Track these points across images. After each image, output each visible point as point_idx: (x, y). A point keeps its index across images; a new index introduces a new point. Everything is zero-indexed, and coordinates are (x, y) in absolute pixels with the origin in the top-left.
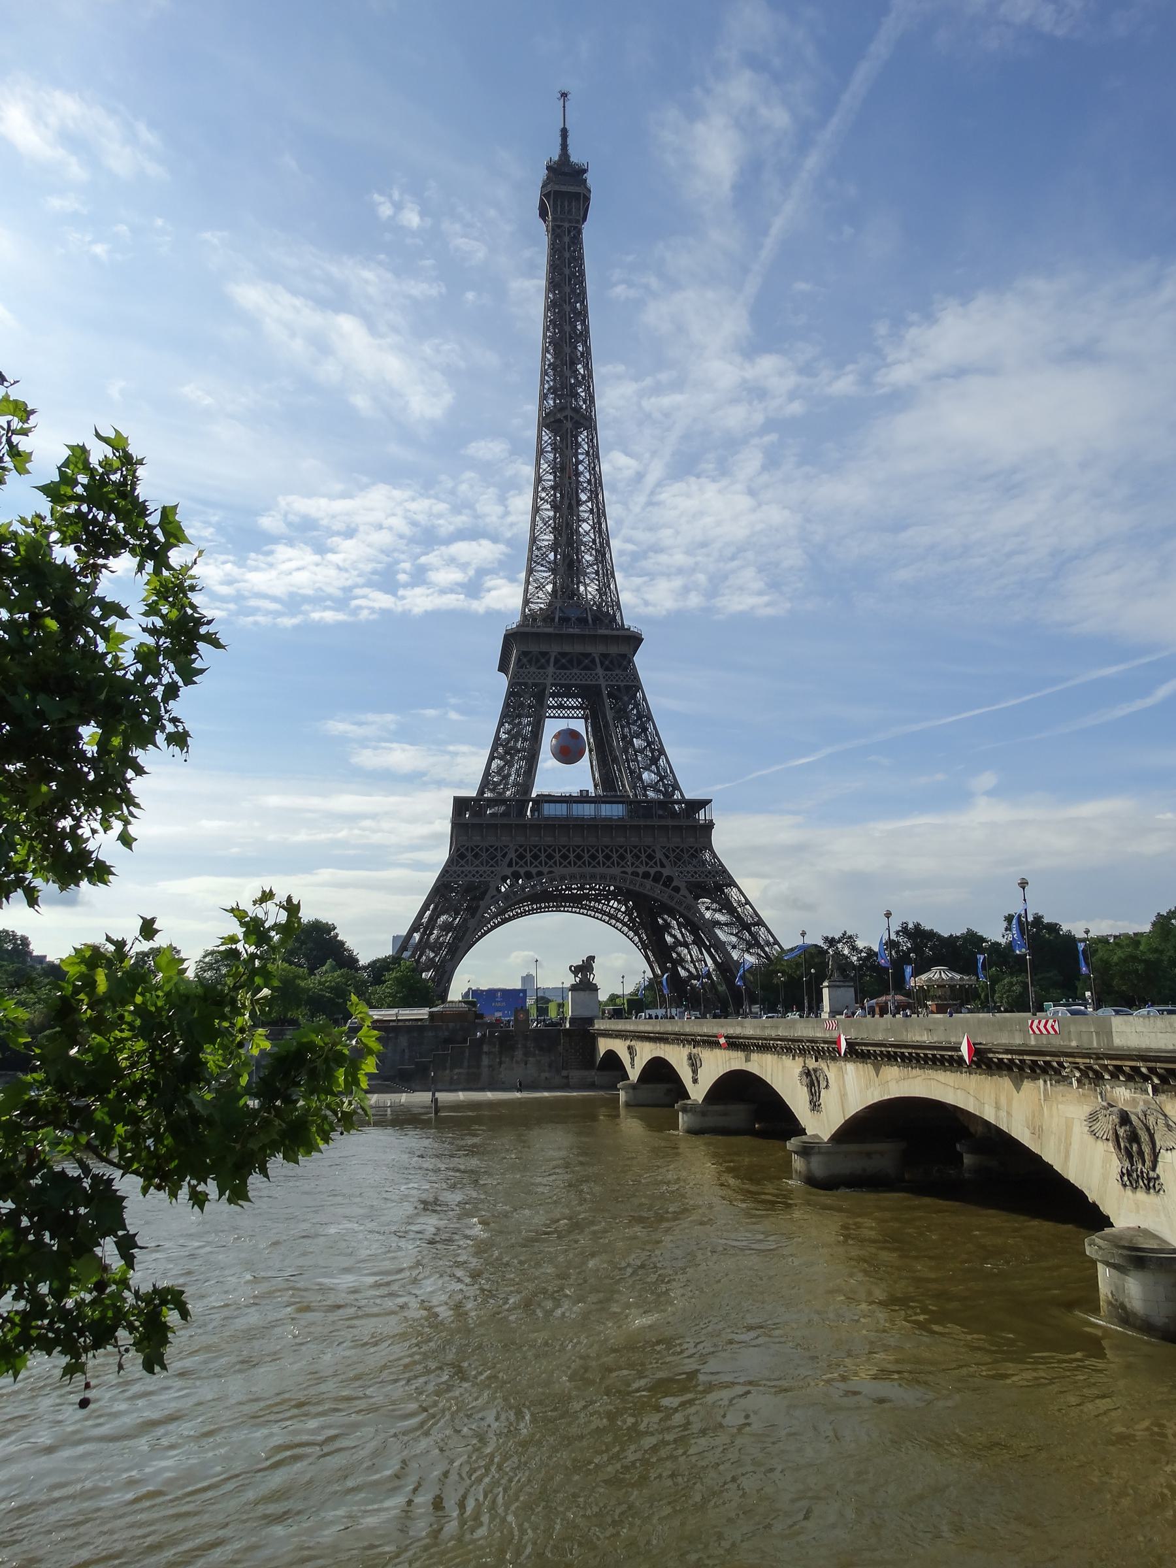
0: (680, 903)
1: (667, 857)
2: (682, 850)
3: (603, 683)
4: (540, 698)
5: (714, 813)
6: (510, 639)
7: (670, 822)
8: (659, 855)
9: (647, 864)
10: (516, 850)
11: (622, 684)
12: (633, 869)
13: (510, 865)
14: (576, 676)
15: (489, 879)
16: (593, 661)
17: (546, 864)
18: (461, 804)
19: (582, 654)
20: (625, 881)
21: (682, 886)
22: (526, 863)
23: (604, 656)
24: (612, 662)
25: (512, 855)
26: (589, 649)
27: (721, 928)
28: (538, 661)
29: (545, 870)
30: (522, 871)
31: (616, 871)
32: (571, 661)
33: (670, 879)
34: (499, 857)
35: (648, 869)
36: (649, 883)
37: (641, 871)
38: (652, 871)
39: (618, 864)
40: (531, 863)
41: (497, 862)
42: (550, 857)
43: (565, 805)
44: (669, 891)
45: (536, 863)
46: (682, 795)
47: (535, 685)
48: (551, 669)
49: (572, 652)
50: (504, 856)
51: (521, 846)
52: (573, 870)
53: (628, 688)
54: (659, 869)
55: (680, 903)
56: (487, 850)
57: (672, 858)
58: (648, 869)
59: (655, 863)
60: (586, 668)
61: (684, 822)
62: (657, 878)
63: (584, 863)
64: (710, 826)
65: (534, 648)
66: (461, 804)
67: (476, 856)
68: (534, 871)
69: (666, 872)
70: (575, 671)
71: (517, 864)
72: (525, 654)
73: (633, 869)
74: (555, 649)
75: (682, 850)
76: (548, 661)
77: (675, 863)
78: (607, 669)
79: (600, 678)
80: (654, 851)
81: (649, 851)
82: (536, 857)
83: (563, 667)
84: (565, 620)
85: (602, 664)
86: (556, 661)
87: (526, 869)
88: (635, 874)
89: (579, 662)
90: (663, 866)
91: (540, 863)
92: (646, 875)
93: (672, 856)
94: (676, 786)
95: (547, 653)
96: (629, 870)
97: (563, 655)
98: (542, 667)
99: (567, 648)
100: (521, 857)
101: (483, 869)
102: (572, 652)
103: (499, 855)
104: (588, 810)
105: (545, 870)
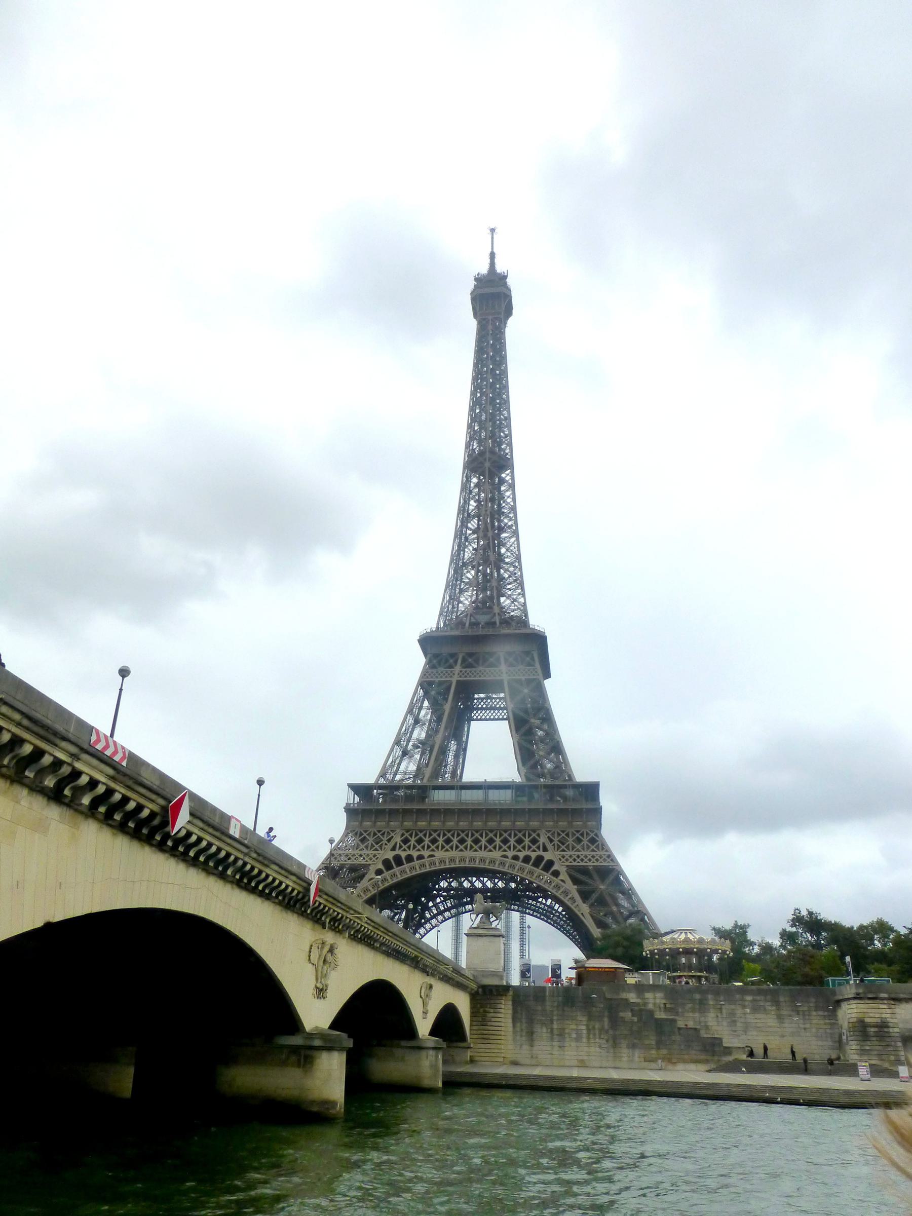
1: (551, 841)
8: (543, 840)
10: (403, 835)
12: (515, 853)
13: (393, 849)
21: (563, 870)
25: (398, 839)
29: (426, 853)
30: (403, 855)
31: (497, 855)
33: (550, 863)
36: (529, 867)
37: (521, 855)
38: (533, 855)
39: (500, 848)
41: (381, 847)
43: (453, 792)
45: (419, 847)
50: (389, 841)
52: (454, 853)
54: (541, 853)
55: (558, 887)
56: (375, 834)
59: (538, 848)
68: (415, 854)
69: (547, 856)
71: (401, 847)
77: (559, 847)
80: (538, 835)
81: (534, 835)
87: (408, 852)
90: (545, 849)
91: (423, 847)
92: (527, 859)
93: (556, 840)
96: (510, 854)
100: (406, 841)
103: (385, 839)
105: (426, 853)
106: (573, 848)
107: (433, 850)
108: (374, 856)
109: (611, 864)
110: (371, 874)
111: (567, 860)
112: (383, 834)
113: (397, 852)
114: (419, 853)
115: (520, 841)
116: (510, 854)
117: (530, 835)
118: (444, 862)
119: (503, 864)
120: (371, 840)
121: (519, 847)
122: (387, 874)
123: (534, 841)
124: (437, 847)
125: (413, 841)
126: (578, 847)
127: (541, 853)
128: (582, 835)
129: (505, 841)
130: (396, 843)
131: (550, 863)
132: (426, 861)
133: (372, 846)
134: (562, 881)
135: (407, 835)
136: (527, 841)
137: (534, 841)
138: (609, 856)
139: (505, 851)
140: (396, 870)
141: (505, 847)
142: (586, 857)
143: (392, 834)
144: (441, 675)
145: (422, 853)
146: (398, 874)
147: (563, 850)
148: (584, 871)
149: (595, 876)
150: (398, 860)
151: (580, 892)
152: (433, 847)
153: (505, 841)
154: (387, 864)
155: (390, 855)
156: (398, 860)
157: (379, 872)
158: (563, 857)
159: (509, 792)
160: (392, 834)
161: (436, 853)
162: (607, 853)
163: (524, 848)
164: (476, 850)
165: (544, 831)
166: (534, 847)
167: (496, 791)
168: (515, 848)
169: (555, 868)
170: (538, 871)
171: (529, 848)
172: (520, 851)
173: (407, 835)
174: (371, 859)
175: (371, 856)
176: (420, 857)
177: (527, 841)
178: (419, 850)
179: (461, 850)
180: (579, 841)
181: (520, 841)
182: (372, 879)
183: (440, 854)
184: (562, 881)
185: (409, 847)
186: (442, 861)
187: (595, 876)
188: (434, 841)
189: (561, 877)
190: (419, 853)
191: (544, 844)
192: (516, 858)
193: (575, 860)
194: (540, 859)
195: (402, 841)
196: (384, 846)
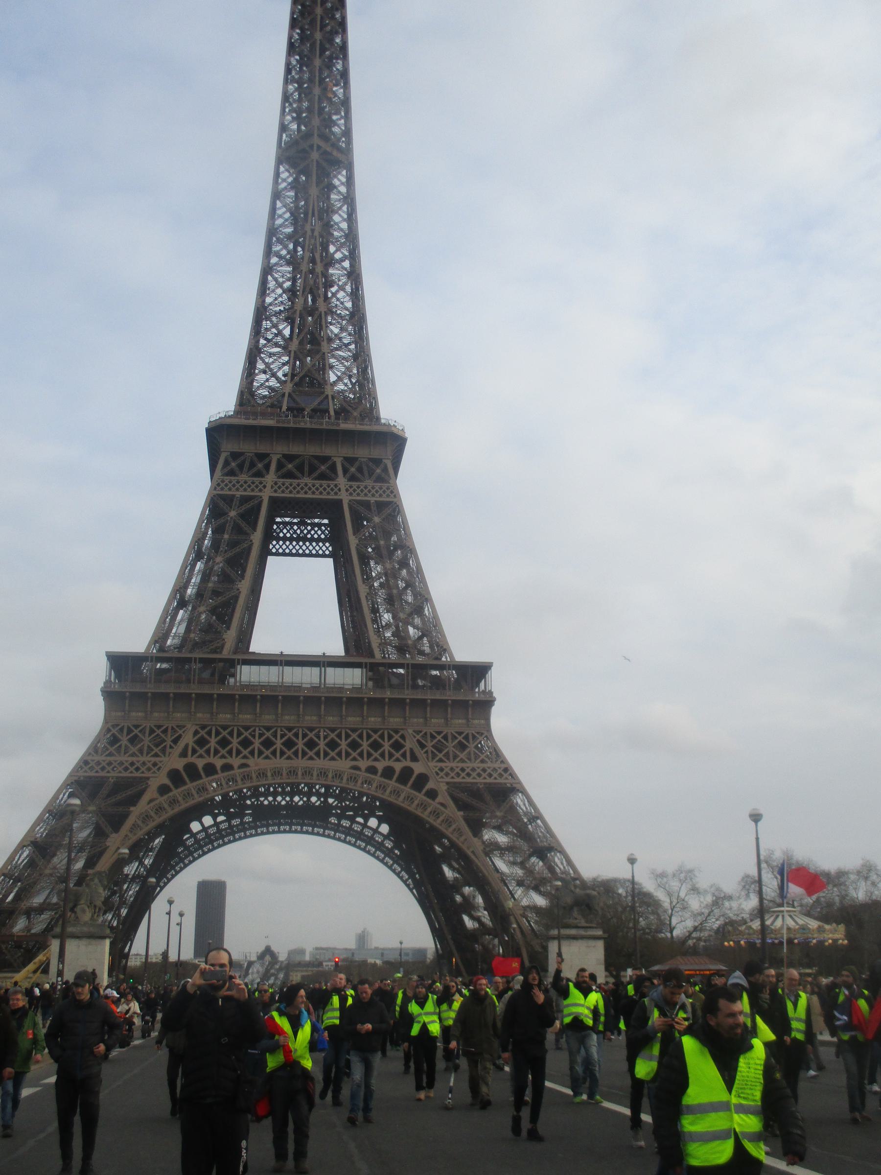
0: (436, 814)
1: (422, 746)
2: (445, 738)
3: (345, 498)
4: (250, 516)
5: (497, 683)
6: (217, 433)
7: (429, 696)
8: (409, 744)
9: (391, 755)
10: (196, 733)
11: (373, 500)
12: (370, 763)
13: (184, 754)
14: (306, 488)
15: (147, 775)
16: (333, 468)
17: (238, 752)
18: (120, 663)
19: (317, 457)
20: (355, 780)
22: (208, 752)
23: (350, 461)
24: (360, 470)
25: (188, 739)
26: (328, 451)
27: (501, 856)
28: (252, 465)
29: (236, 762)
30: (200, 763)
31: (343, 765)
32: (300, 468)
33: (422, 780)
34: (169, 742)
35: (391, 763)
36: (392, 783)
37: (380, 766)
38: (398, 767)
39: (348, 755)
40: (216, 752)
41: (164, 751)
42: (246, 743)
43: (274, 669)
44: (421, 797)
45: (223, 752)
46: (451, 656)
47: (245, 500)
48: (271, 478)
49: (301, 454)
50: (175, 741)
51: (203, 727)
53: (381, 506)
54: (408, 763)
55: (436, 814)
56: (152, 731)
57: (429, 744)
58: (391, 763)
59: (404, 755)
60: (323, 477)
61: (449, 695)
62: (405, 775)
63: (296, 754)
64: (486, 704)
65: (249, 448)
66: (120, 663)
67: (133, 740)
68: (219, 763)
69: (418, 768)
70: (306, 480)
71: (194, 751)
72: (235, 456)
73: (370, 763)
74: (277, 450)
75: (445, 738)
76: (267, 467)
77: (434, 756)
78: (353, 478)
79: (343, 490)
81: (396, 737)
82: (224, 743)
83: (290, 475)
84: (296, 411)
85: (345, 471)
86: (280, 466)
88: (372, 770)
89: (312, 469)
90: (414, 758)
91: (230, 753)
92: (388, 773)
93: (429, 744)
94: (441, 648)
95: (267, 455)
96: (363, 764)
97: (290, 458)
98: (259, 474)
99: (295, 449)
100: (202, 742)
101: (142, 759)
102: (301, 454)
104: (308, 677)
105: (236, 762)
106: (455, 757)
107: (245, 757)
108: (155, 764)
109: (510, 780)
110: (151, 793)
111: (447, 774)
112: (165, 731)
113: (190, 759)
114: (224, 761)
115: (376, 746)
116: (363, 764)
117: (390, 737)
118: (264, 775)
119: (353, 779)
120: (147, 740)
121: (376, 755)
122: (176, 792)
123: (397, 746)
124: (252, 753)
125: (213, 742)
126: (462, 755)
127: (408, 763)
128: (466, 738)
129: (354, 745)
130: (187, 746)
131: (422, 780)
132: (237, 771)
133: (150, 749)
134: (442, 804)
135: (203, 733)
136: (386, 746)
137: (397, 746)
138: (506, 770)
139: (354, 759)
140: (191, 786)
141: (354, 754)
142: (473, 770)
143: (181, 732)
144: (242, 486)
145: (229, 760)
146: (194, 792)
147: (441, 760)
148: (474, 792)
149: (488, 797)
150: (192, 772)
151: (467, 820)
152: (246, 752)
153: (354, 745)
154: (175, 777)
155: (179, 764)
156: (192, 772)
157: (163, 790)
158: (441, 770)
159: (358, 672)
160: (181, 732)
161: (251, 761)
162: (503, 766)
163: (382, 755)
164: (311, 758)
165: (410, 731)
166: (398, 755)
167: (339, 670)
168: (369, 755)
169: (430, 785)
170: (407, 790)
171: (391, 755)
172: (376, 760)
173: (203, 733)
174: (149, 769)
175: (149, 765)
176: (227, 767)
177: (386, 746)
178: (223, 757)
179: (289, 758)
180: (462, 747)
181: (376, 746)
182: (151, 801)
183: (256, 763)
184: (442, 804)
185: (208, 752)
186: (262, 774)
187: (488, 797)
188: (246, 743)
189: (439, 799)
190: (224, 761)
191: (411, 750)
192: (372, 770)
193: (458, 775)
194: (407, 773)
195: (195, 742)
196: (168, 750)
